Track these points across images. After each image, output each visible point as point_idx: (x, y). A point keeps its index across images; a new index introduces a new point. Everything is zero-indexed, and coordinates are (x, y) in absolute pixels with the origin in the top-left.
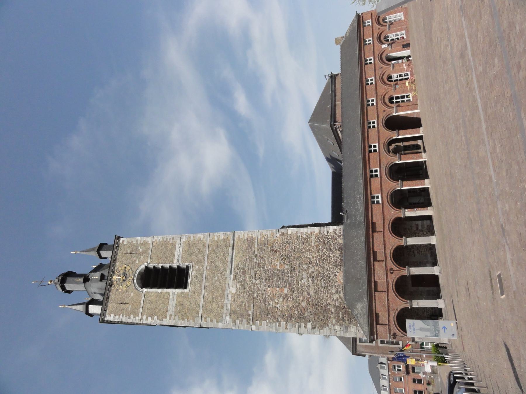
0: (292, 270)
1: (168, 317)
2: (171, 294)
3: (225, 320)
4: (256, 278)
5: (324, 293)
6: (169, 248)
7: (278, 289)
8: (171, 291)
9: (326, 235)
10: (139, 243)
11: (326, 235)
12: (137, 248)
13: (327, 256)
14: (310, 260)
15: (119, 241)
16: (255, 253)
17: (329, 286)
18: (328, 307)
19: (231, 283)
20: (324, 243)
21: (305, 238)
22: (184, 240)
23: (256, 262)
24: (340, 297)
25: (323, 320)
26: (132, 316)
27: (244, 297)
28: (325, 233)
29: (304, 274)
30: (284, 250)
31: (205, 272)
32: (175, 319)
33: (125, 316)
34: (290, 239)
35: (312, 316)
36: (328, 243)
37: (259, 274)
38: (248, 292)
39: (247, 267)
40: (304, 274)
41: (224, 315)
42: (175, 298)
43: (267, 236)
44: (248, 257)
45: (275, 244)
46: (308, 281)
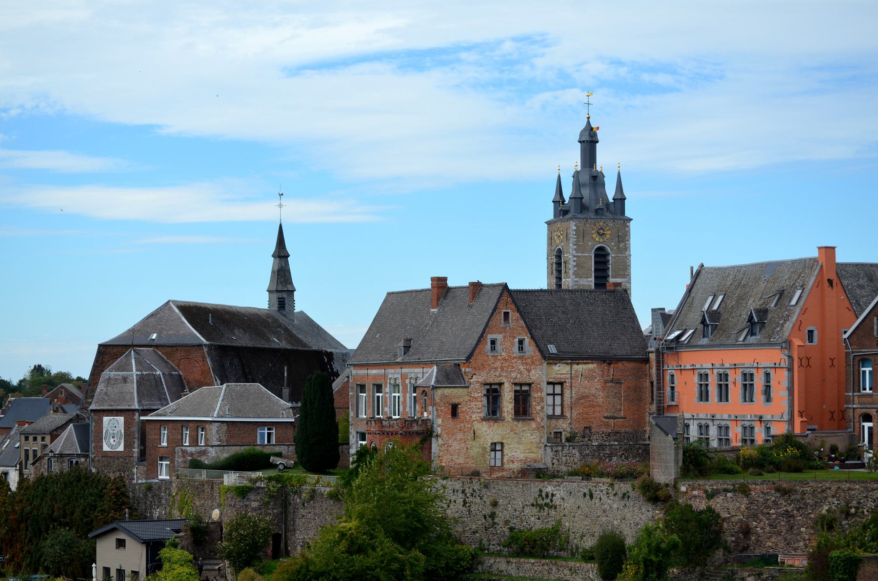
1: (576, 279)
2: (591, 279)
6: (622, 273)
10: (627, 242)
12: (623, 242)
26: (575, 247)
32: (575, 285)
33: (575, 240)
42: (588, 283)
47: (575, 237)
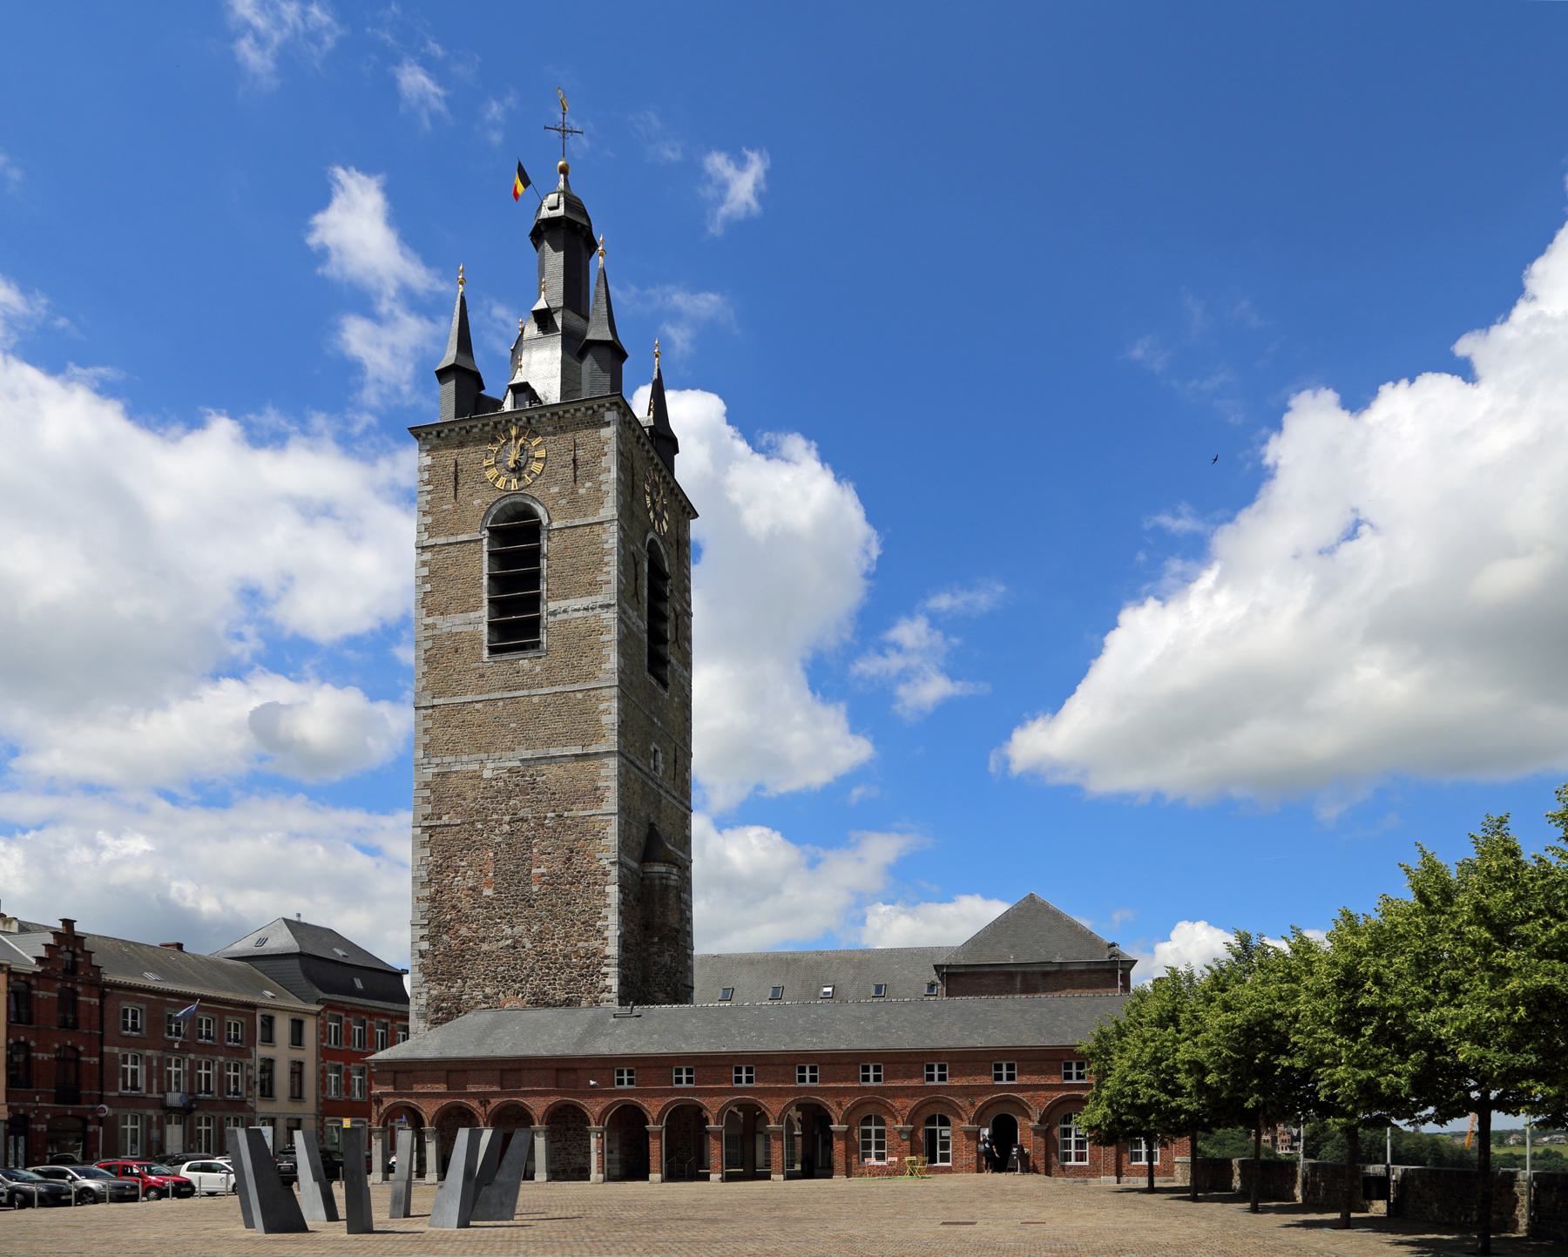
0: (529, 901)
1: (429, 621)
2: (477, 614)
3: (429, 764)
4: (513, 822)
5: (485, 971)
7: (491, 874)
8: (484, 612)
9: (599, 971)
11: (599, 971)
13: (555, 975)
14: (548, 939)
15: (609, 409)
16: (566, 813)
17: (497, 981)
18: (459, 981)
19: (502, 765)
20: (582, 969)
21: (595, 926)
22: (604, 616)
23: (545, 818)
24: (477, 1003)
25: (436, 972)
27: (475, 799)
28: (605, 970)
29: (519, 929)
30: (570, 879)
31: (525, 692)
34: (593, 892)
35: (442, 949)
36: (582, 975)
37: (521, 827)
38: (484, 809)
39: (537, 798)
40: (519, 929)
41: (437, 760)
42: (470, 628)
43: (603, 838)
44: (557, 796)
45: (585, 859)
46: (507, 939)
47: (430, 488)
